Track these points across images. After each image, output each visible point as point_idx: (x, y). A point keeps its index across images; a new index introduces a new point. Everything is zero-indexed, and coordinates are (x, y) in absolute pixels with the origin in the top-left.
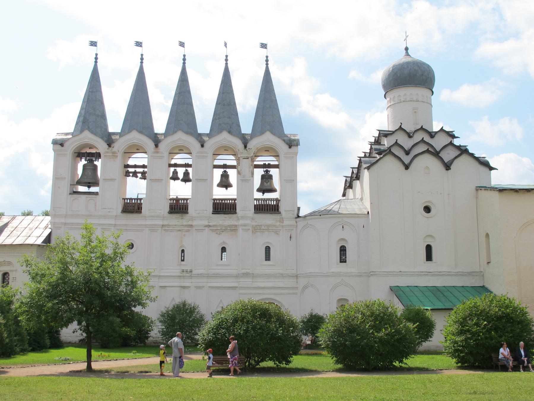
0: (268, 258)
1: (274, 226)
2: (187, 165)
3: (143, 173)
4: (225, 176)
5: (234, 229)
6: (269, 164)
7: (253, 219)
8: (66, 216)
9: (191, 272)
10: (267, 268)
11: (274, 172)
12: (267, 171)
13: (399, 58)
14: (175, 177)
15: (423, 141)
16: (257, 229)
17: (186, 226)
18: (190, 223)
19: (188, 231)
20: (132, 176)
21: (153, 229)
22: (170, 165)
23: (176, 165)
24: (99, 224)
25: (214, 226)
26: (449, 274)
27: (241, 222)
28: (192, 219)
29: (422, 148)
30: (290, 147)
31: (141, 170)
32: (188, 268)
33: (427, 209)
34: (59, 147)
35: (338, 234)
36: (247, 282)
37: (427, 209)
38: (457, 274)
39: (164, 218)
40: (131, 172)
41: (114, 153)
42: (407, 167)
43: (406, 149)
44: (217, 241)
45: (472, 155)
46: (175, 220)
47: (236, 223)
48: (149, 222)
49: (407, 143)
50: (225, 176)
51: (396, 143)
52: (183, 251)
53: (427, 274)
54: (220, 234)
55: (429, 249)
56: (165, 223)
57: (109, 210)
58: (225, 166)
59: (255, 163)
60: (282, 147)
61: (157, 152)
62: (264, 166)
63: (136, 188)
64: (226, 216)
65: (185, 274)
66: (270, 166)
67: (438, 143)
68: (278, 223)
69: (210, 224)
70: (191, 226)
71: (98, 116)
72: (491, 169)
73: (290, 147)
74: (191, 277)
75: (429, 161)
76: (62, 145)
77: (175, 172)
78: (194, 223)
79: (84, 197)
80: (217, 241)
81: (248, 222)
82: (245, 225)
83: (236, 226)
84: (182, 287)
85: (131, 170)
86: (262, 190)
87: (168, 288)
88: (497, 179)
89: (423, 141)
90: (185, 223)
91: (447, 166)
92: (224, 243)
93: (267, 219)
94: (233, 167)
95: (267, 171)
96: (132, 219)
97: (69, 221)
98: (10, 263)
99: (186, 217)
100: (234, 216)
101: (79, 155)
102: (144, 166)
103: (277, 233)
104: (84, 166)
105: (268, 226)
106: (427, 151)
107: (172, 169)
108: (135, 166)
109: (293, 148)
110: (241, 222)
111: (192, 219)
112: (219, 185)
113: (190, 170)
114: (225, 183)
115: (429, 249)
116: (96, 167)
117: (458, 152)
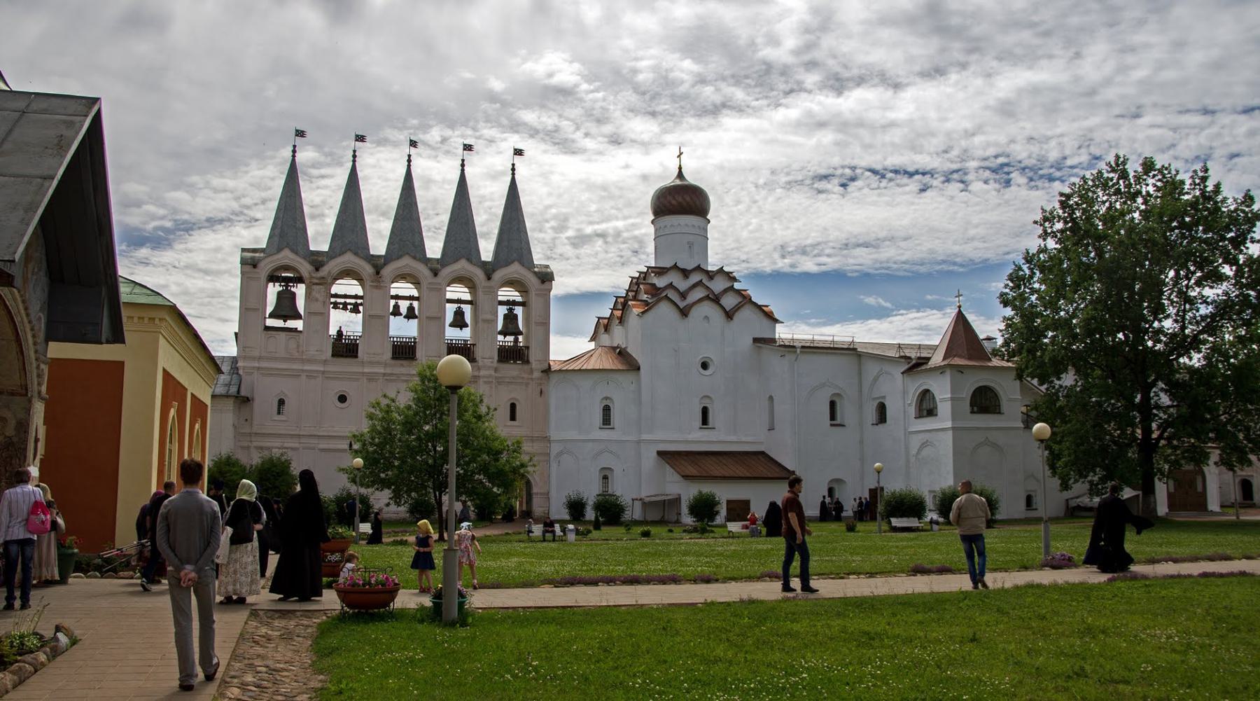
0: (513, 418)
2: (411, 298)
3: (356, 306)
4: (459, 314)
8: (260, 358)
11: (519, 311)
12: (511, 310)
13: (670, 180)
14: (396, 312)
15: (700, 283)
16: (500, 382)
20: (352, 311)
23: (397, 297)
24: (303, 371)
30: (543, 282)
31: (353, 301)
33: (705, 366)
34: (248, 268)
37: (705, 366)
39: (386, 365)
45: (755, 304)
49: (682, 285)
50: (459, 314)
51: (671, 286)
55: (705, 411)
56: (388, 371)
59: (500, 298)
60: (533, 281)
63: (344, 322)
66: (514, 303)
67: (718, 285)
72: (776, 321)
73: (543, 282)
75: (708, 309)
76: (255, 266)
77: (396, 307)
79: (283, 334)
86: (504, 333)
91: (729, 315)
93: (512, 370)
95: (511, 310)
96: (345, 365)
97: (264, 364)
101: (273, 278)
102: (356, 297)
104: (279, 293)
106: (707, 298)
108: (345, 296)
109: (546, 285)
113: (415, 304)
114: (459, 322)
115: (705, 411)
116: (294, 294)
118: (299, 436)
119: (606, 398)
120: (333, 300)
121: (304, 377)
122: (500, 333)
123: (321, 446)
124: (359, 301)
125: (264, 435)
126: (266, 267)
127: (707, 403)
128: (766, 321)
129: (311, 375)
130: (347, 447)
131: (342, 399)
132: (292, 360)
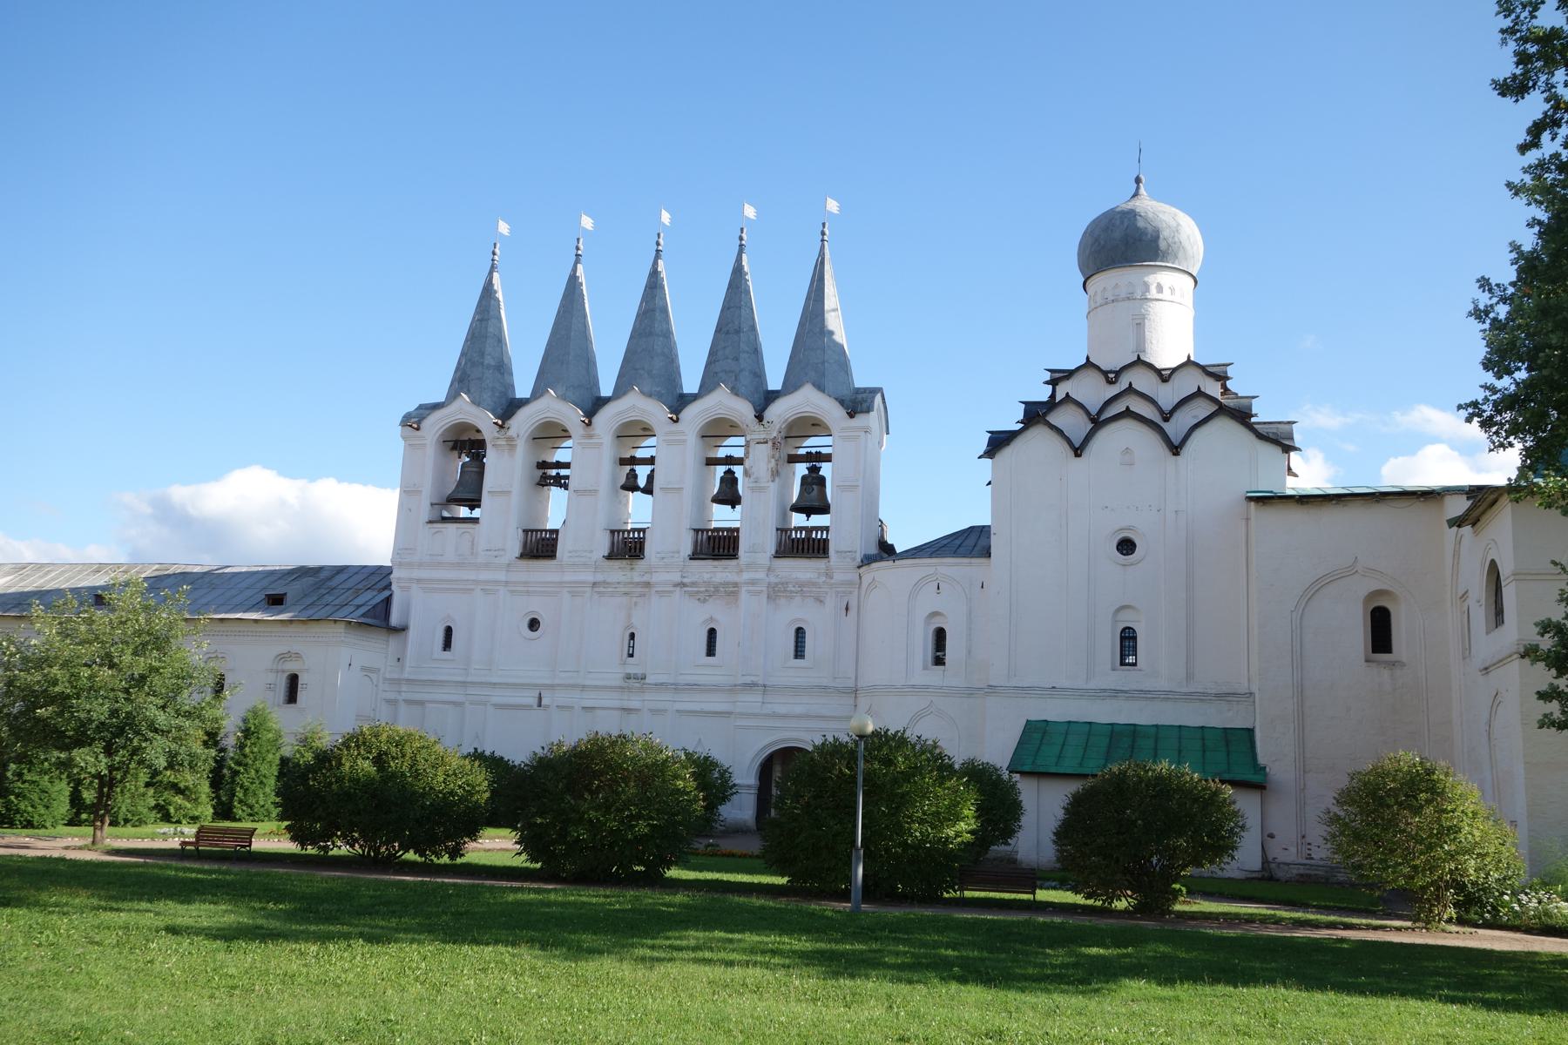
0: (799, 652)
1: (814, 584)
5: (731, 592)
6: (818, 453)
9: (644, 678)
10: (798, 673)
12: (814, 470)
14: (631, 485)
16: (776, 592)
17: (638, 584)
18: (645, 579)
19: (642, 595)
22: (712, 462)
24: (476, 582)
25: (693, 584)
26: (1168, 696)
27: (746, 576)
29: (1201, 409)
35: (929, 601)
36: (751, 701)
38: (1190, 697)
39: (596, 568)
40: (551, 477)
41: (510, 439)
42: (1078, 452)
43: (1094, 411)
46: (619, 572)
48: (568, 577)
52: (632, 636)
53: (1116, 693)
54: (705, 601)
56: (600, 577)
58: (729, 460)
61: (591, 437)
62: (809, 458)
64: (716, 563)
70: (648, 584)
71: (489, 367)
73: (851, 415)
77: (633, 476)
78: (655, 578)
80: (697, 618)
81: (761, 575)
82: (753, 582)
83: (736, 585)
85: (553, 472)
87: (598, 712)
88: (1309, 473)
89: (1199, 393)
90: (637, 579)
93: (802, 569)
94: (740, 462)
95: (814, 470)
96: (541, 571)
97: (424, 574)
98: (298, 656)
99: (640, 564)
100: (734, 562)
103: (820, 601)
105: (802, 585)
107: (720, 470)
109: (860, 420)
110: (746, 576)
112: (718, 500)
117: (1214, 408)
118: (464, 684)
119: (935, 614)
120: (553, 472)
122: (797, 508)
123: (495, 700)
124: (563, 472)
125: (433, 683)
126: (435, 426)
127: (1127, 619)
128: (1270, 452)
130: (534, 702)
132: (459, 565)
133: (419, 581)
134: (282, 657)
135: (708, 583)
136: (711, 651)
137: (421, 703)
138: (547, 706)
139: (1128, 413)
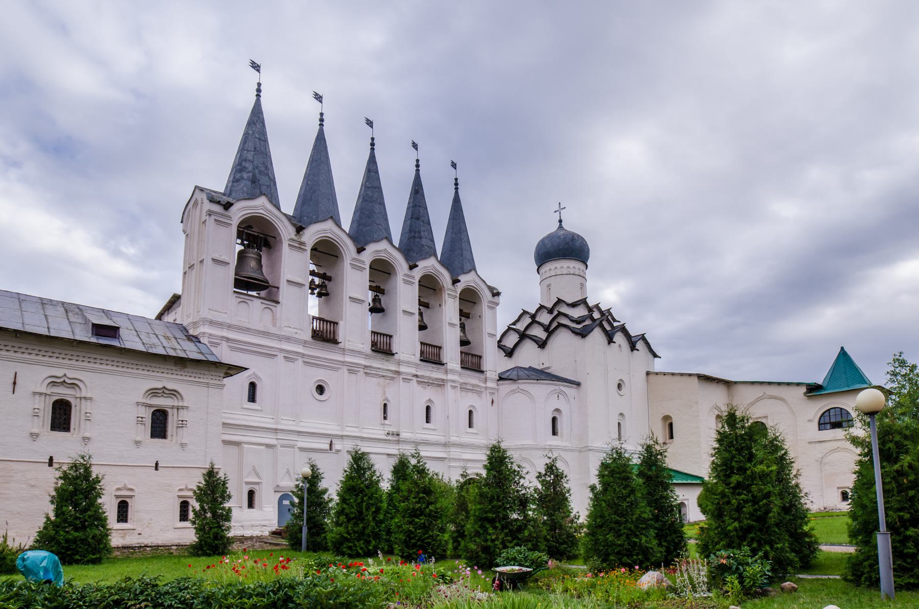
5: (440, 384)
7: (460, 375)
9: (398, 435)
10: (468, 437)
19: (392, 379)
21: (353, 369)
24: (281, 350)
25: (423, 377)
27: (450, 377)
28: (399, 363)
32: (395, 430)
39: (367, 356)
44: (423, 395)
46: (378, 363)
47: (444, 377)
48: (348, 359)
52: (385, 405)
57: (295, 331)
65: (390, 438)
68: (482, 384)
69: (418, 373)
70: (398, 373)
74: (398, 442)
78: (403, 369)
82: (454, 381)
84: (388, 455)
92: (430, 400)
98: (174, 393)
105: (474, 385)
109: (496, 299)
111: (399, 363)
118: (276, 431)
121: (281, 356)
123: (300, 444)
129: (290, 357)
130: (328, 447)
131: (321, 389)
133: (228, 340)
134: (154, 392)
135: (429, 378)
136: (428, 420)
137: (237, 444)
138: (338, 451)
139: (560, 325)
